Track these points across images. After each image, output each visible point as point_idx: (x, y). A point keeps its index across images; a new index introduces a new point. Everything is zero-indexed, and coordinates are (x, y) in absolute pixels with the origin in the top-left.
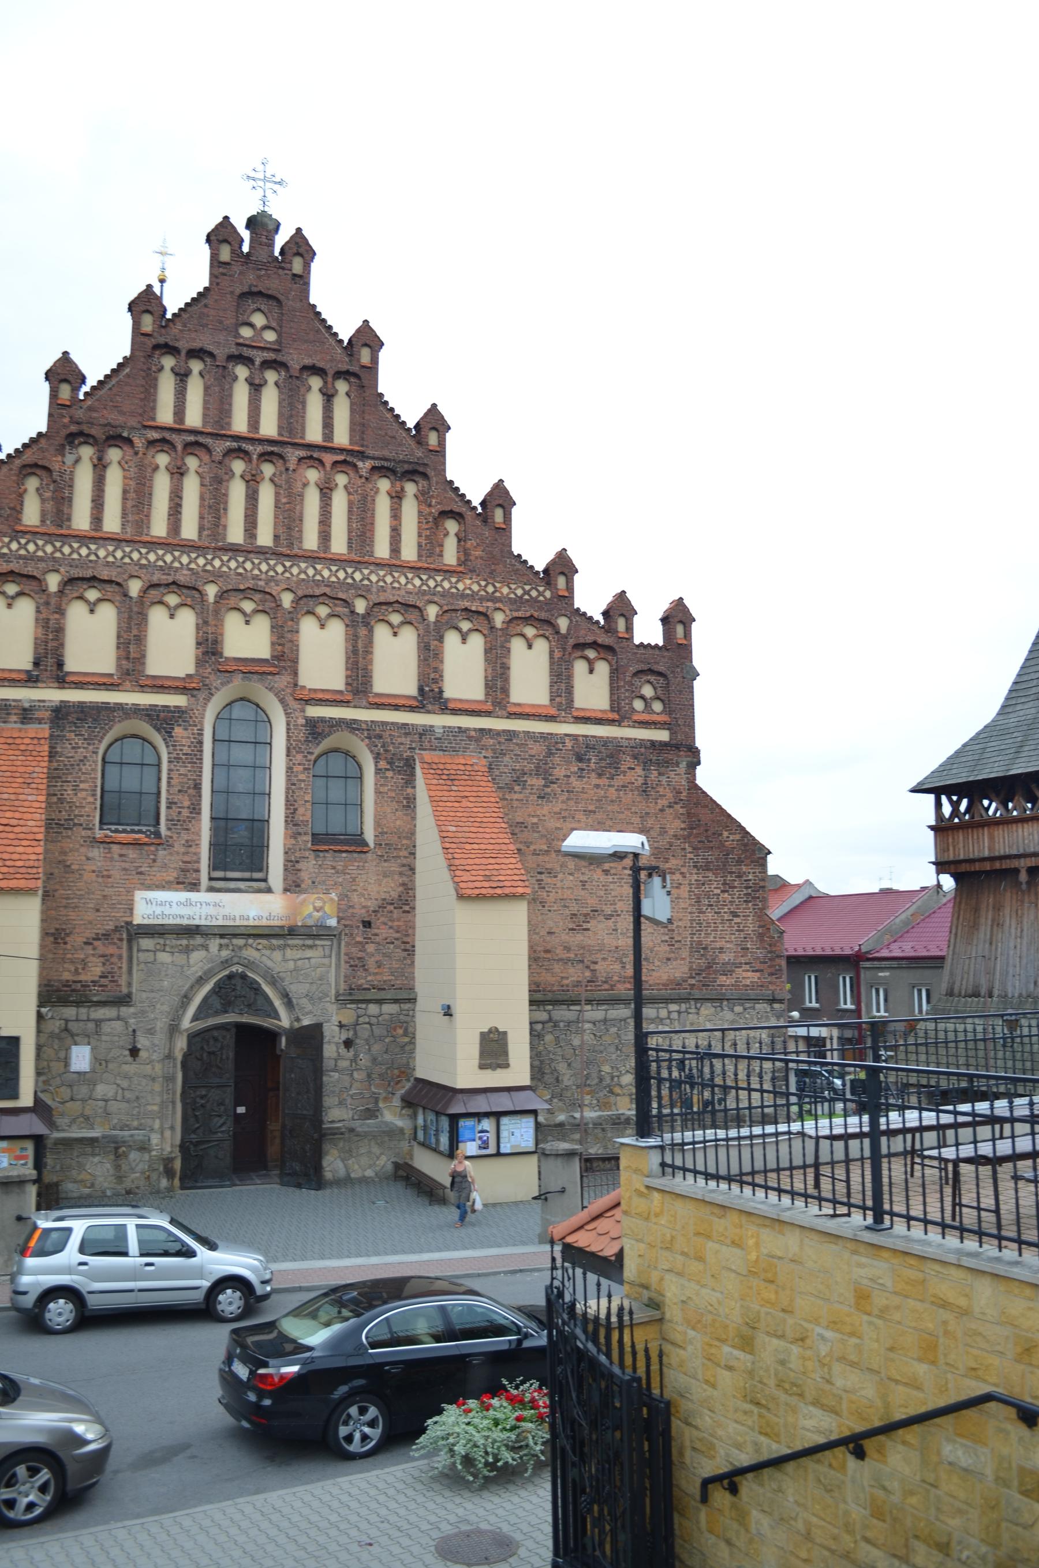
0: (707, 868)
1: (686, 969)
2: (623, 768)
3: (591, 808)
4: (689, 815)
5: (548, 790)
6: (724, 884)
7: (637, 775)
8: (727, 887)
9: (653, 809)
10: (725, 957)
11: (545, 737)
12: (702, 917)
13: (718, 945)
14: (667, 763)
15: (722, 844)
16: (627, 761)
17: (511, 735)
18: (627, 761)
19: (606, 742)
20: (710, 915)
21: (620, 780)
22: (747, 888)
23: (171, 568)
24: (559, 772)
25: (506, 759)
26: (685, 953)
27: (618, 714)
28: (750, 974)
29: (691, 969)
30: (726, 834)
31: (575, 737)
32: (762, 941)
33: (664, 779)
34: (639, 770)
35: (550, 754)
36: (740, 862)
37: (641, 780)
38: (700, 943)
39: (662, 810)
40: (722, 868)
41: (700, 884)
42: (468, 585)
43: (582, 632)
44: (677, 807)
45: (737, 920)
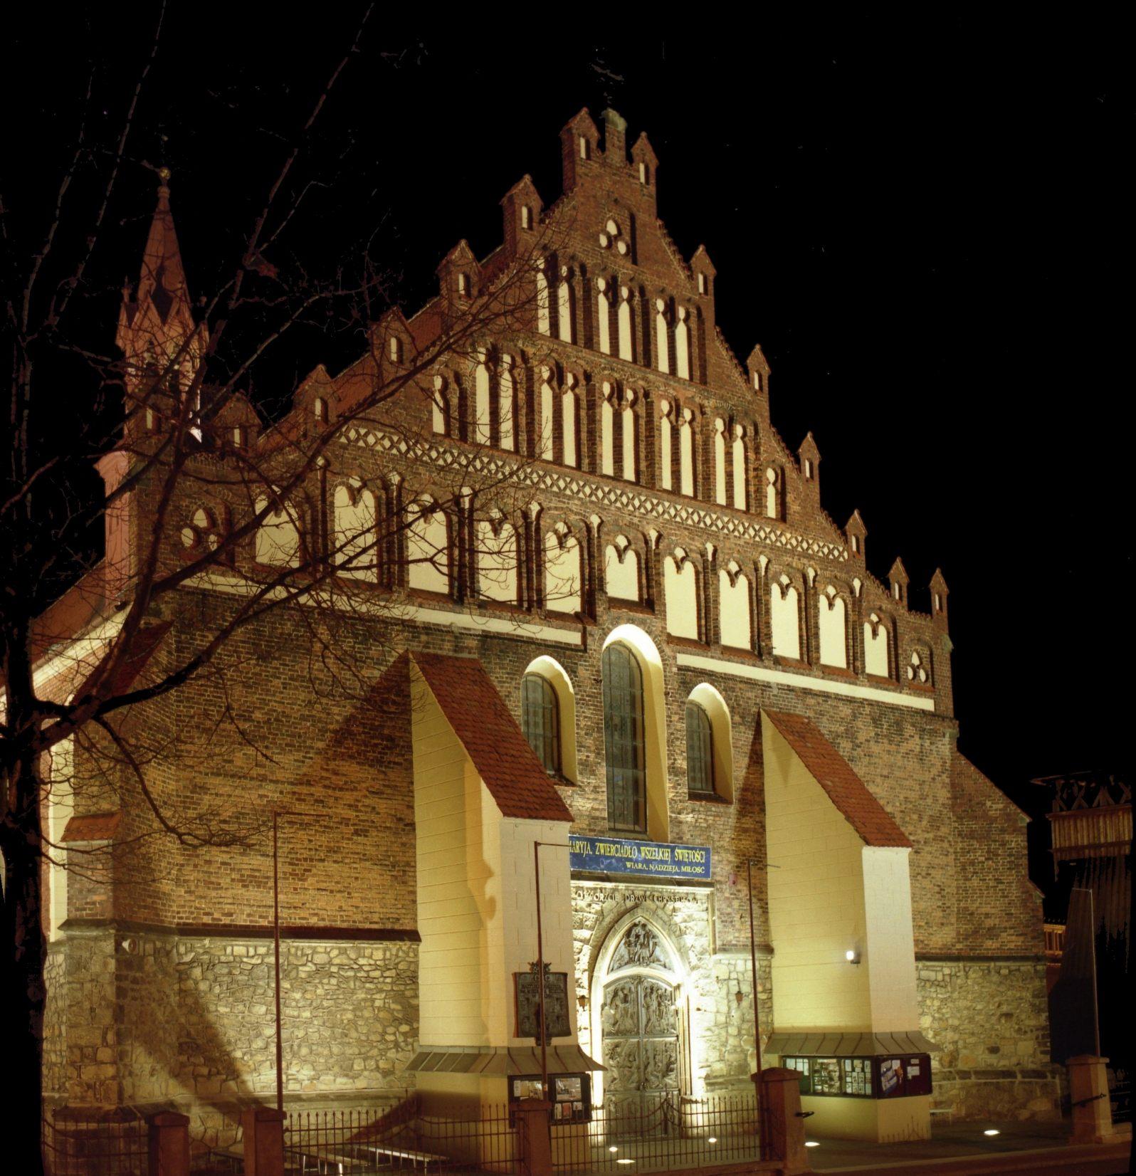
0: (971, 835)
1: (954, 934)
2: (907, 735)
3: (885, 773)
4: (953, 785)
5: (855, 753)
6: (988, 852)
7: (914, 744)
8: (992, 855)
9: (927, 777)
10: (989, 923)
11: (850, 700)
12: (968, 884)
13: (984, 910)
14: (933, 733)
15: (985, 816)
16: (909, 730)
17: (826, 696)
18: (909, 730)
19: (894, 708)
20: (975, 882)
21: (905, 747)
22: (1010, 855)
23: (565, 495)
24: (862, 737)
25: (824, 719)
26: (953, 920)
27: (895, 679)
28: (1014, 938)
29: (958, 933)
30: (989, 804)
31: (871, 703)
32: (1025, 906)
33: (933, 747)
34: (917, 737)
35: (855, 716)
36: (1003, 831)
37: (918, 749)
38: (966, 909)
39: (934, 779)
40: (984, 837)
41: (965, 852)
42: (788, 538)
43: (872, 597)
44: (944, 776)
45: (1001, 886)
